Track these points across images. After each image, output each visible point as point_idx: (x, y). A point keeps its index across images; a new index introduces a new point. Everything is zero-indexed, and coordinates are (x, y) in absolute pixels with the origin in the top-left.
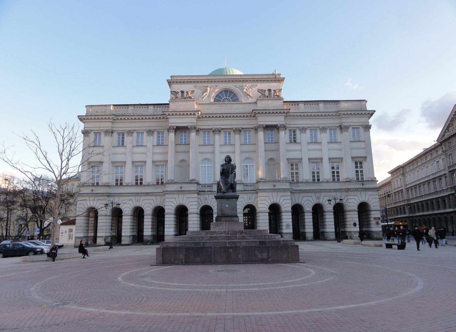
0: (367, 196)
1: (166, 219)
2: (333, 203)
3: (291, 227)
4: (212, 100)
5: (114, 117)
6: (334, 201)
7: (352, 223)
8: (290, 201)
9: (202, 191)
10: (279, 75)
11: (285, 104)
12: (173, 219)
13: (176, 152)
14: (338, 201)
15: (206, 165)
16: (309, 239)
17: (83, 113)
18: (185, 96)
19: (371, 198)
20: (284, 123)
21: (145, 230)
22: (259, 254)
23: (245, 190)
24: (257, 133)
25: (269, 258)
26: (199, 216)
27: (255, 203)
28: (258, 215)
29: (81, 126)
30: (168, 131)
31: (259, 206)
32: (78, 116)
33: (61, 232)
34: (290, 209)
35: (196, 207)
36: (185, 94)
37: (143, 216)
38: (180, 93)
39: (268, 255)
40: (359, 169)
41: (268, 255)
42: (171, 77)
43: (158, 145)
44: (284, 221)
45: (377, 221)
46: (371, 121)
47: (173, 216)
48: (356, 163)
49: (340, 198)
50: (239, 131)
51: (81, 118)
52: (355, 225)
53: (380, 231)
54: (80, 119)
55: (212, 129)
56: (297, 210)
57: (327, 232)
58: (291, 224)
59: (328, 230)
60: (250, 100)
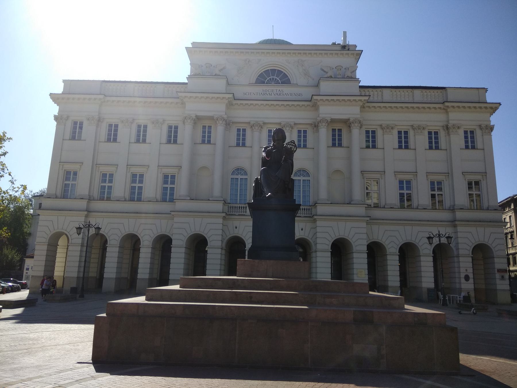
1: (172, 255)
2: (436, 241)
5: (102, 97)
6: (437, 239)
7: (463, 275)
8: (365, 236)
9: (229, 215)
10: (356, 46)
12: (183, 255)
14: (444, 240)
15: (239, 177)
17: (59, 89)
20: (359, 116)
24: (318, 131)
26: (224, 252)
28: (314, 255)
29: (55, 109)
31: (319, 241)
32: (51, 94)
33: (26, 267)
34: (365, 248)
35: (220, 238)
42: (193, 43)
45: (502, 274)
46: (494, 119)
47: (183, 250)
49: (447, 235)
51: (54, 97)
52: (467, 278)
54: (52, 98)
55: (249, 123)
56: (375, 251)
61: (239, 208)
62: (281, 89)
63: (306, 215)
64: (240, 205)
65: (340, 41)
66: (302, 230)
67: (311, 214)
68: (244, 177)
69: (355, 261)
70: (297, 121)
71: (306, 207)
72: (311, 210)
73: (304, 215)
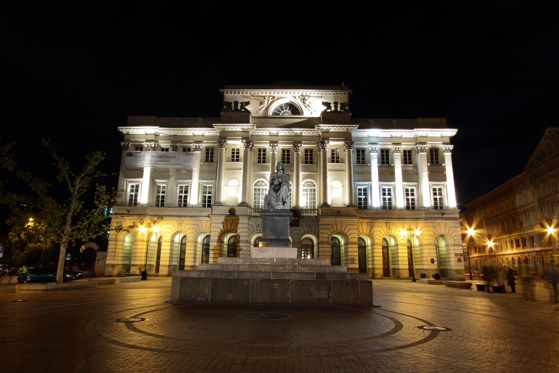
0: (447, 228)
3: (357, 262)
7: (430, 259)
16: (378, 277)
18: (239, 108)
19: (452, 230)
22: (316, 292)
25: (329, 297)
36: (239, 105)
38: (233, 105)
39: (329, 294)
41: (329, 294)
45: (460, 257)
52: (432, 261)
53: (462, 270)
57: (399, 269)
58: (357, 258)
59: (401, 267)
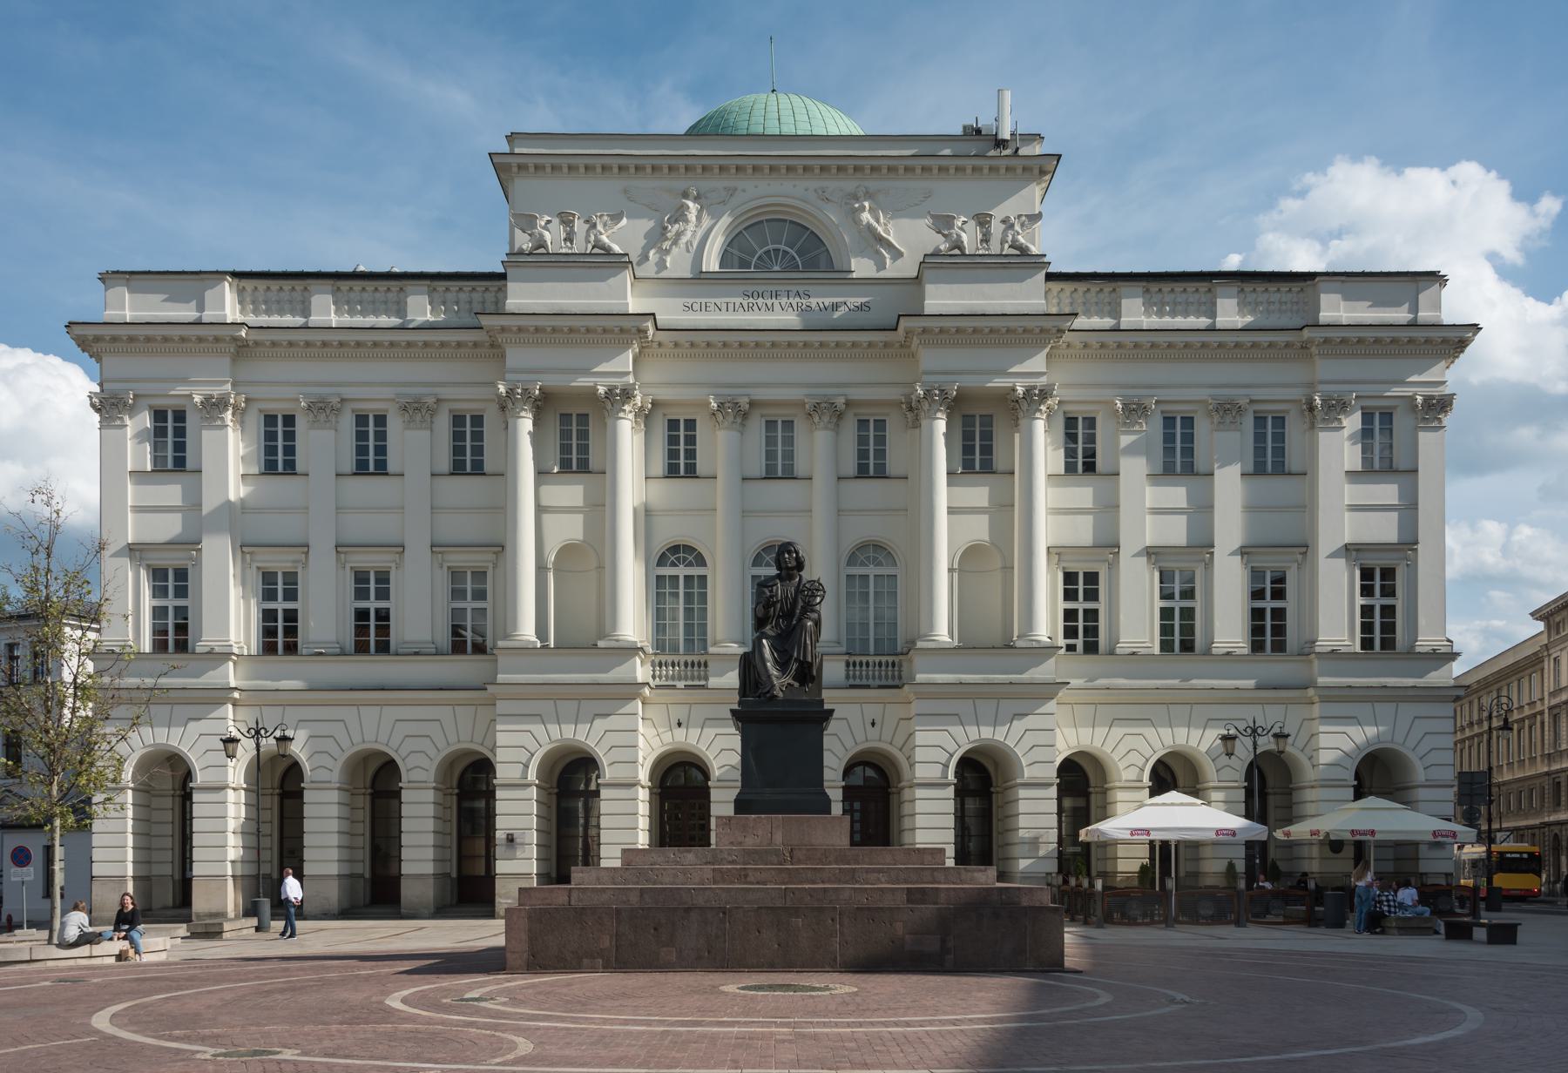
1: (500, 807)
4: (712, 263)
11: (1055, 286)
13: (540, 509)
15: (681, 571)
21: (405, 854)
23: (852, 687)
24: (916, 424)
27: (899, 741)
30: (503, 408)
31: (919, 754)
34: (1051, 773)
37: (397, 794)
40: (1377, 601)
43: (458, 469)
44: (1023, 821)
48: (1367, 574)
50: (830, 411)
60: (892, 270)
61: (686, 664)
62: (801, 289)
63: (884, 682)
64: (689, 659)
65: (986, 122)
66: (873, 724)
67: (900, 677)
68: (696, 571)
69: (1023, 806)
70: (857, 394)
71: (884, 659)
72: (900, 666)
73: (878, 682)
